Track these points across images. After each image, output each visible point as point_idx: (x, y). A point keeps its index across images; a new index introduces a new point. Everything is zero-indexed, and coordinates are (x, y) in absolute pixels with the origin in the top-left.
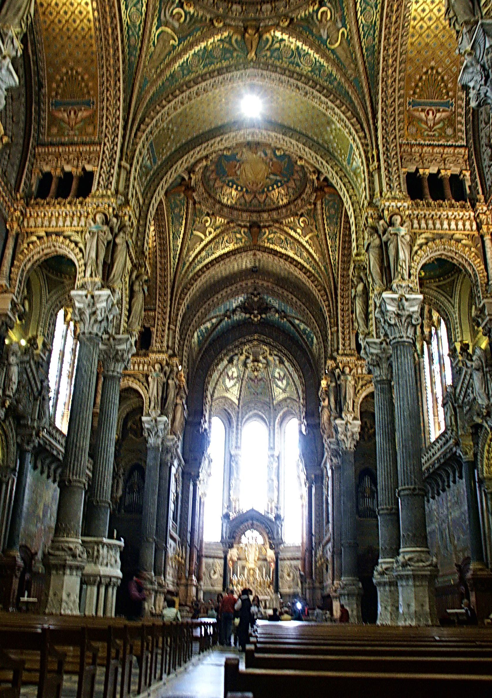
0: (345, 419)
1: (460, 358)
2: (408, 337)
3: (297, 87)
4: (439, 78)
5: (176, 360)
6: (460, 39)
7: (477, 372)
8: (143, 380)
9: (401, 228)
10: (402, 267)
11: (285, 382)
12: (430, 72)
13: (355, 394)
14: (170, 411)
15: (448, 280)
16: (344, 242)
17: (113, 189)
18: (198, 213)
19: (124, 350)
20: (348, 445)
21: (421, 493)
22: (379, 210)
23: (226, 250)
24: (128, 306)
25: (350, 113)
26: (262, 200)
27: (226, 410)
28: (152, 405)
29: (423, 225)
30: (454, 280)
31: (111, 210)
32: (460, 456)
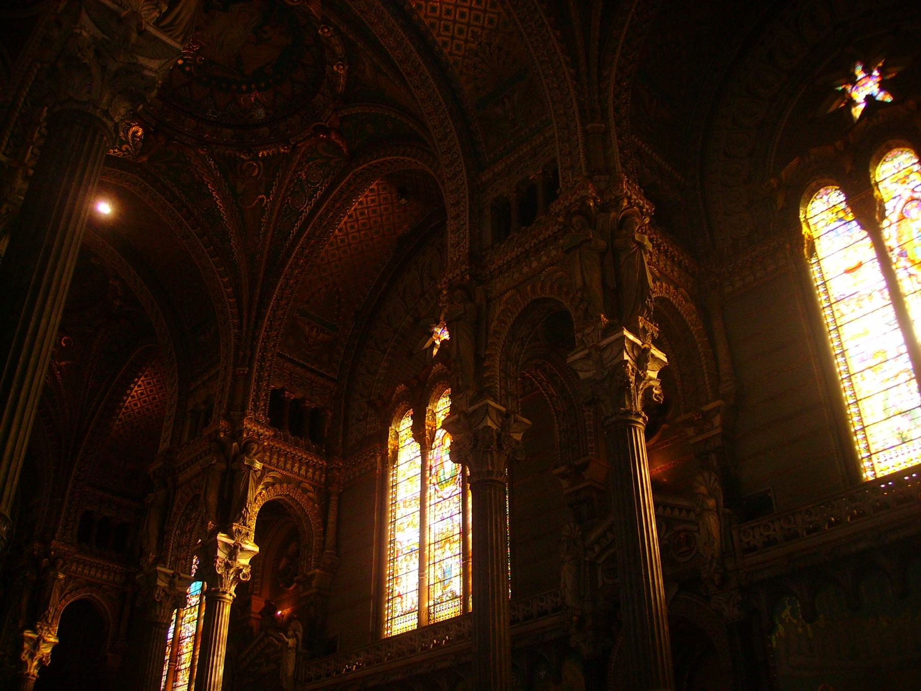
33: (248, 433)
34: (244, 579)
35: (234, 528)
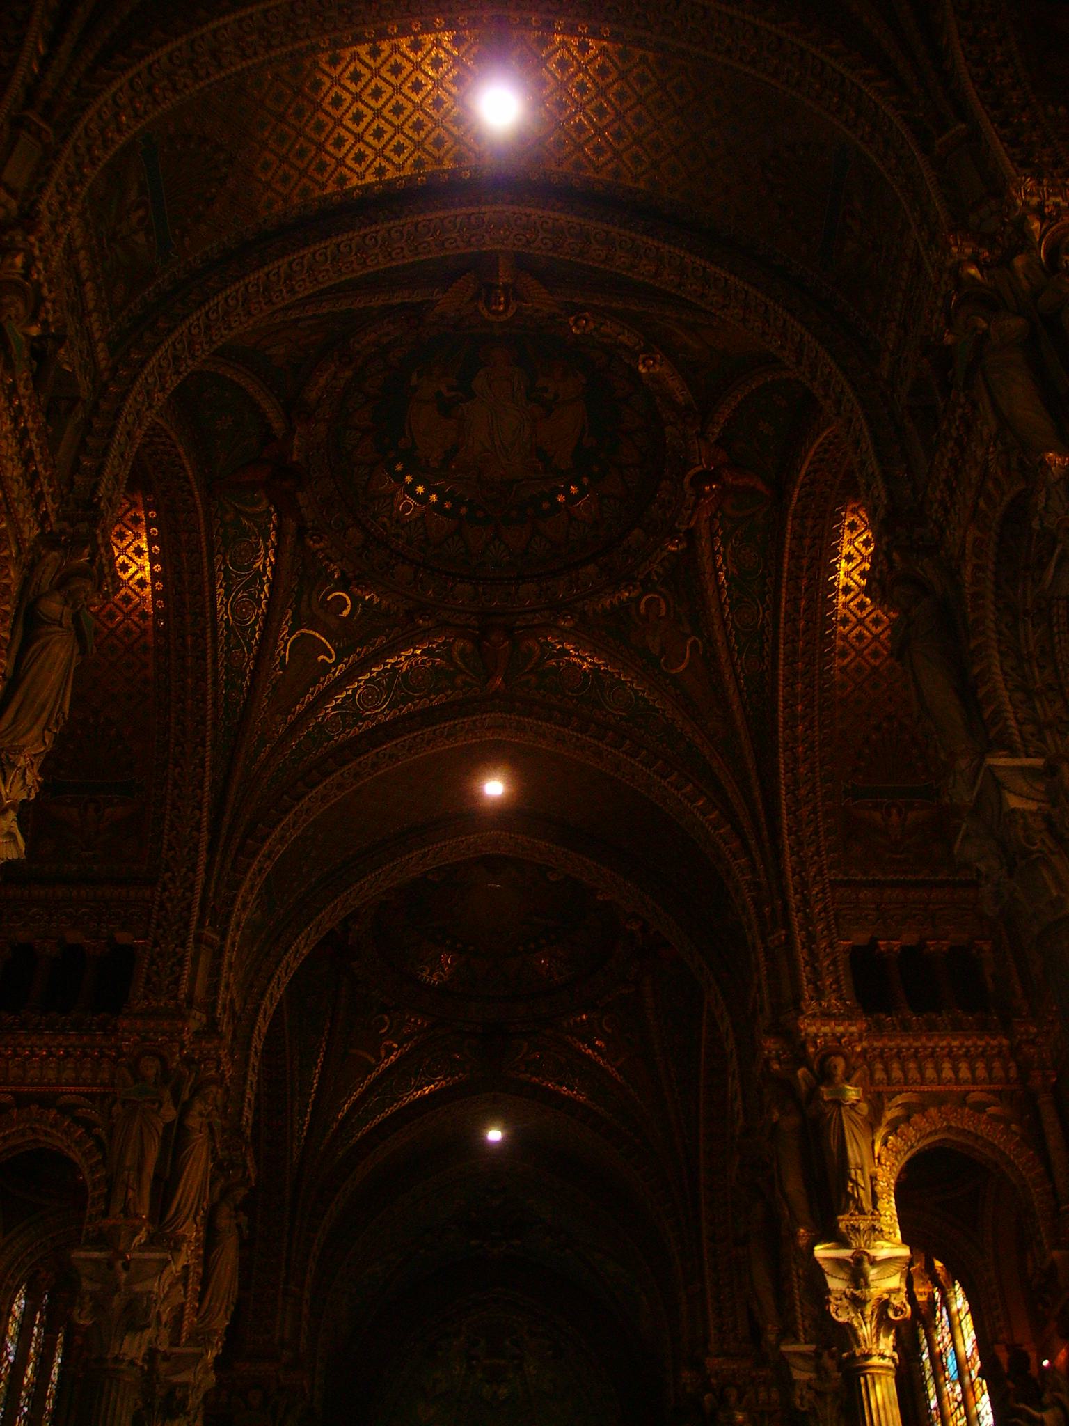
1: (1010, 1385)
2: (883, 1356)
10: (856, 1183)
19: (187, 1384)
29: (897, 1074)
33: (816, 1043)
34: (898, 1318)
35: (842, 1225)
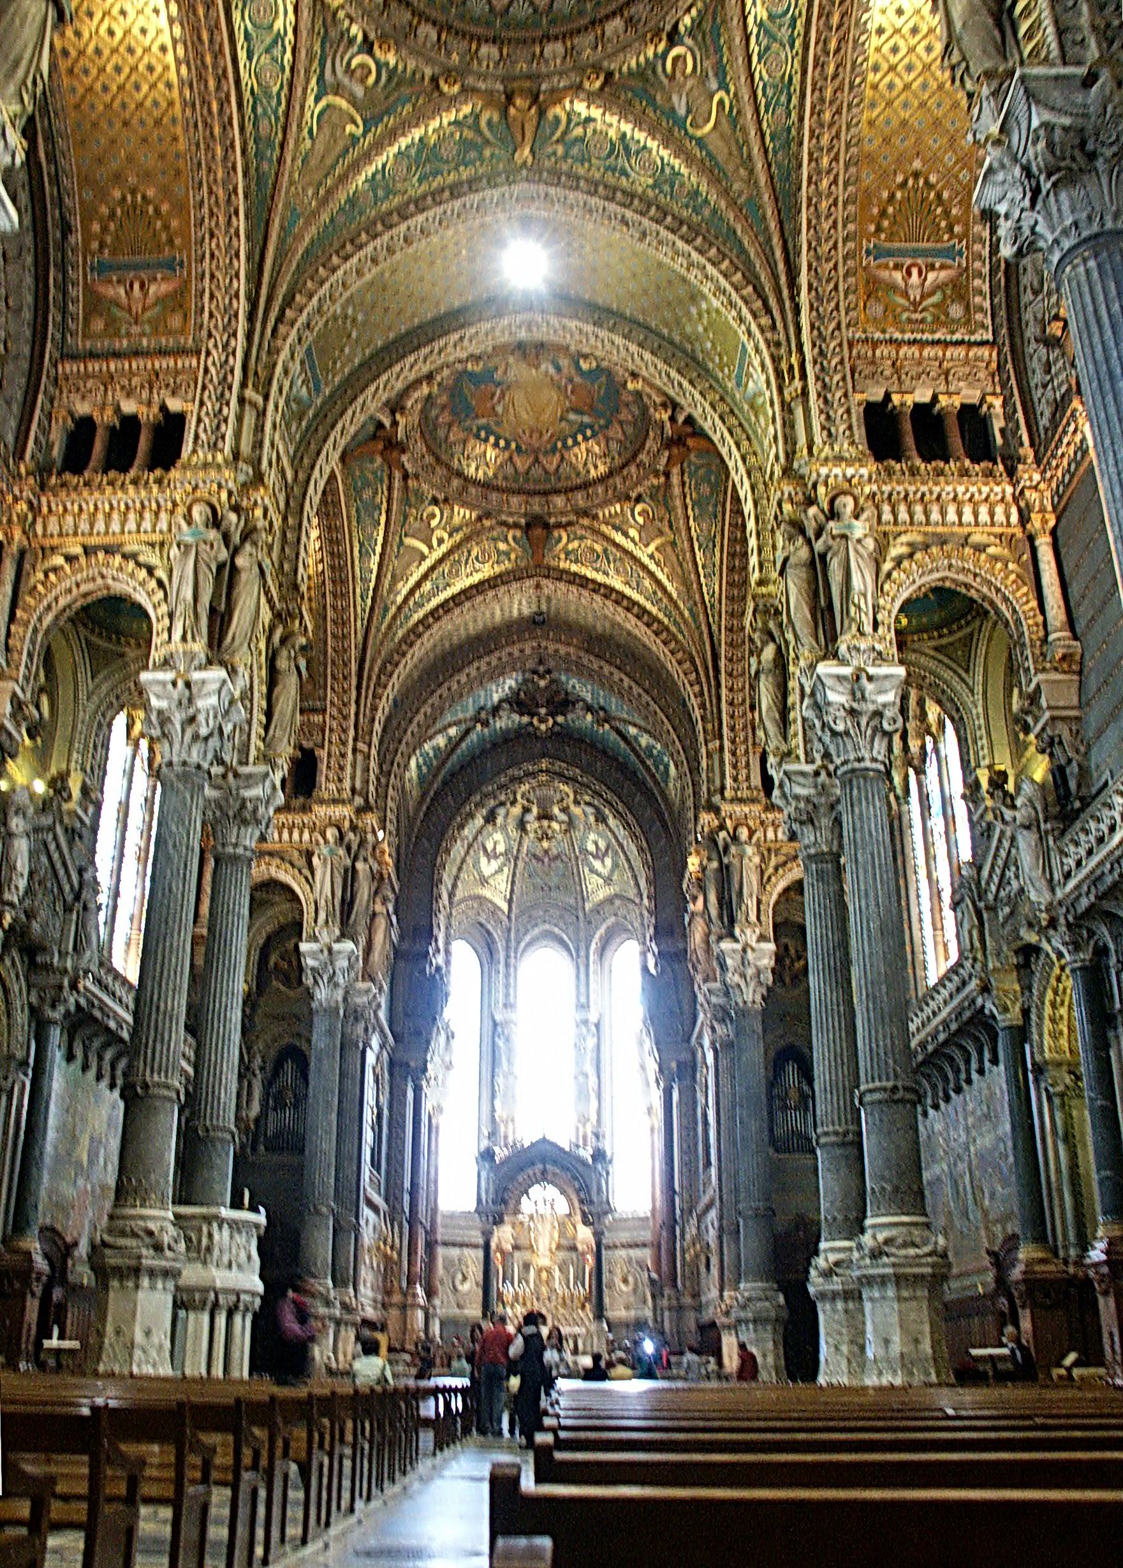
0: (742, 939)
1: (989, 803)
2: (874, 760)
3: (624, 222)
4: (932, 195)
5: (371, 819)
6: (976, 111)
7: (1025, 832)
8: (302, 862)
9: (855, 523)
10: (859, 607)
11: (608, 861)
12: (911, 182)
13: (762, 885)
14: (362, 929)
15: (960, 634)
16: (732, 555)
17: (227, 449)
18: (413, 499)
19: (258, 799)
20: (749, 997)
21: (910, 1096)
22: (806, 485)
23: (476, 578)
24: (264, 704)
25: (739, 275)
26: (552, 468)
27: (481, 925)
28: (322, 916)
29: (903, 515)
30: (971, 634)
31: (224, 496)
32: (993, 1017)
